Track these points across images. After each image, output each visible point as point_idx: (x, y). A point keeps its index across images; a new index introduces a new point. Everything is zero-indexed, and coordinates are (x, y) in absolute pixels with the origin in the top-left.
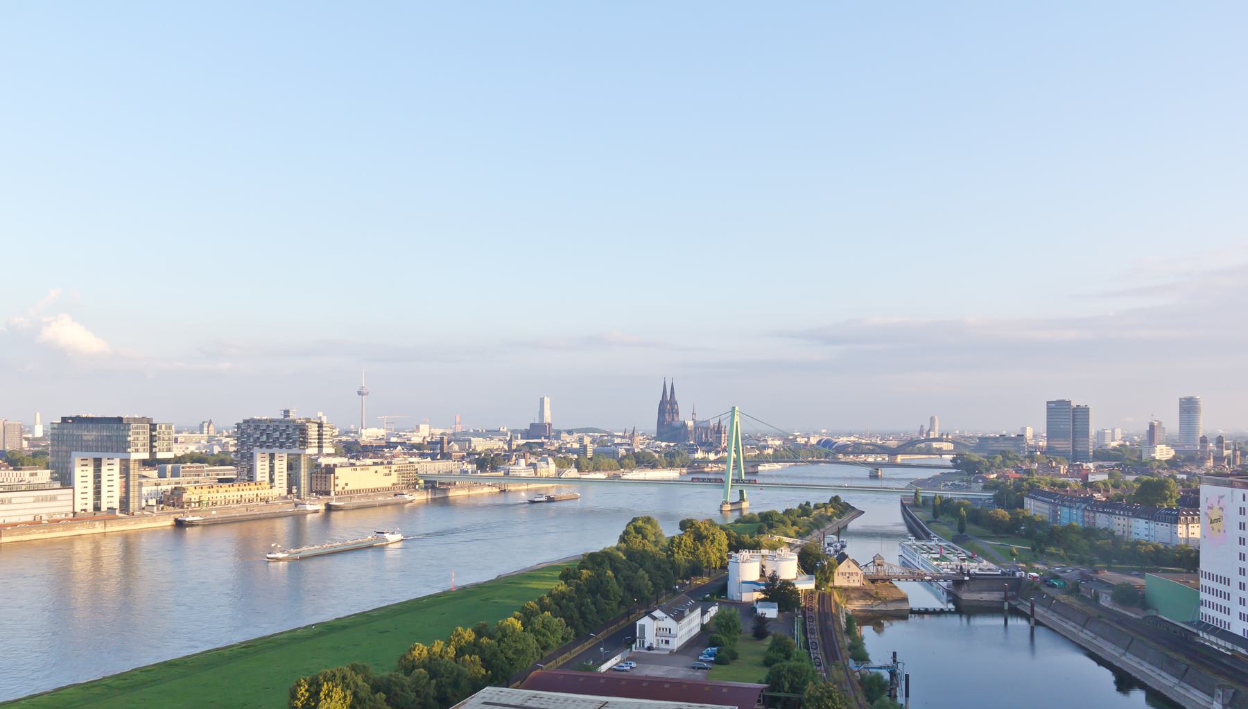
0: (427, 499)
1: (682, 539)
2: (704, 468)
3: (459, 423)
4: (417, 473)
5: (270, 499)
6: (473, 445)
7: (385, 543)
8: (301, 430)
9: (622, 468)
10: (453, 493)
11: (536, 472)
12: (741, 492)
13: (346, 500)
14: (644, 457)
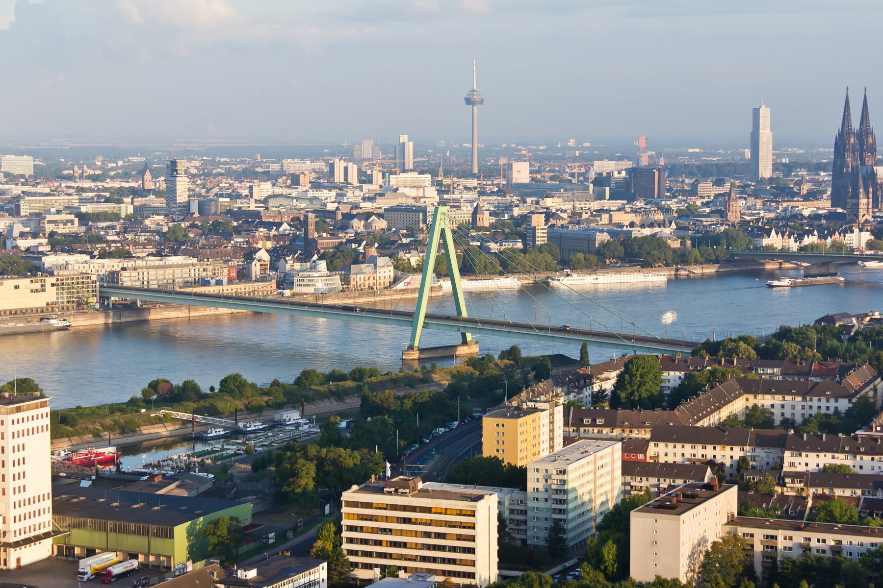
0: (106, 324)
2: (764, 264)
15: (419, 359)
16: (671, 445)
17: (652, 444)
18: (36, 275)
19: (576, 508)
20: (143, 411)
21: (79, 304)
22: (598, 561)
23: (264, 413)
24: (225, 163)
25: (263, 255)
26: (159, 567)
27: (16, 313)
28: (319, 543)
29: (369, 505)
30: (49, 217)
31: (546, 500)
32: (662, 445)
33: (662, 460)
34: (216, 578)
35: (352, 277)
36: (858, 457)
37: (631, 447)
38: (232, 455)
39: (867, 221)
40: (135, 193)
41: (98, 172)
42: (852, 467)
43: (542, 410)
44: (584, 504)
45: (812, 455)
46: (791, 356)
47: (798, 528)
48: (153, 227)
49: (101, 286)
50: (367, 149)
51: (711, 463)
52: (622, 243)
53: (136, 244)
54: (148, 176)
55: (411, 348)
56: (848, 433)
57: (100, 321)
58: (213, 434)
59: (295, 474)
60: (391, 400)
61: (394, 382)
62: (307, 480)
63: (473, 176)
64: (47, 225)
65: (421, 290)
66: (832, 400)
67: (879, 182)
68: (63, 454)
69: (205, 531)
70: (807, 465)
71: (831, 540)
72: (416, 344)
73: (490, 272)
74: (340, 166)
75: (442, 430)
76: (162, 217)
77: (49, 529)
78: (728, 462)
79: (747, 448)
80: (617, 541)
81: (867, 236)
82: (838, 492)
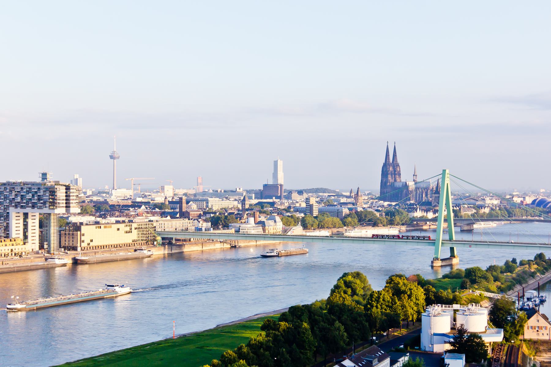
1: (381, 294)
2: (422, 226)
3: (201, 184)
4: (155, 230)
5: (24, 254)
6: (210, 205)
7: (114, 295)
8: (50, 192)
9: (345, 226)
10: (187, 249)
11: (264, 230)
12: (452, 249)
13: (91, 254)
14: (366, 216)
55: (437, 259)
67: (410, 190)
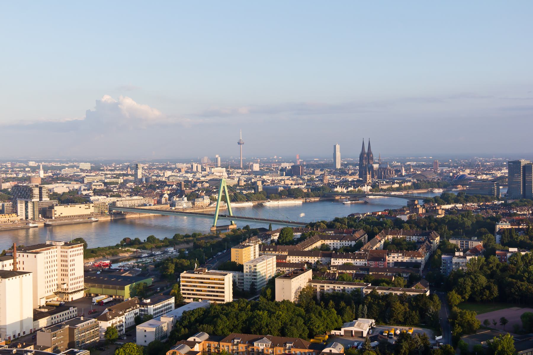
2: (335, 197)
12: (231, 222)
15: (216, 230)
16: (294, 257)
17: (288, 257)
18: (87, 203)
19: (260, 278)
20: (120, 248)
21: (102, 213)
22: (264, 295)
23: (162, 249)
24: (157, 165)
25: (166, 196)
26: (120, 300)
27: (80, 216)
28: (173, 291)
29: (189, 278)
30: (94, 184)
31: (250, 275)
32: (291, 257)
33: (291, 262)
34: (136, 302)
35: (196, 203)
36: (355, 260)
37: (278, 257)
38: (149, 263)
39: (370, 182)
40: (124, 175)
41: (113, 168)
42: (353, 263)
43: (251, 246)
44: (263, 276)
45: (340, 260)
46: (338, 227)
47: (331, 283)
48: (129, 186)
49: (109, 207)
50: (206, 159)
51: (307, 263)
52: (287, 191)
53: (123, 192)
54: (129, 169)
55: (213, 226)
56: (352, 252)
57: (109, 218)
58: (144, 256)
59: (167, 268)
60: (203, 243)
61: (206, 238)
62: (171, 270)
63: (240, 168)
64: (93, 186)
65: (217, 207)
66: (350, 242)
68: (92, 263)
69: (135, 287)
70: (339, 263)
71: (342, 287)
72: (215, 225)
73: (241, 201)
74: (195, 165)
75: (220, 253)
76: (132, 183)
77: (83, 288)
78: (313, 262)
79: (319, 258)
80: (271, 288)
81: (369, 188)
82: (348, 272)
